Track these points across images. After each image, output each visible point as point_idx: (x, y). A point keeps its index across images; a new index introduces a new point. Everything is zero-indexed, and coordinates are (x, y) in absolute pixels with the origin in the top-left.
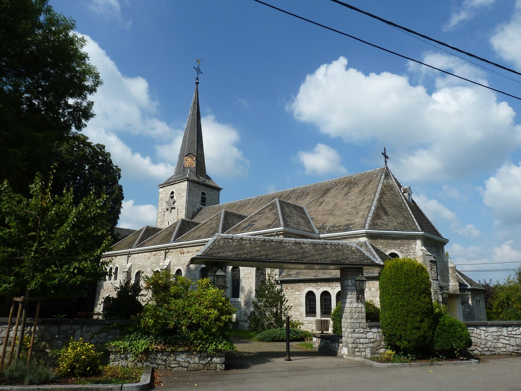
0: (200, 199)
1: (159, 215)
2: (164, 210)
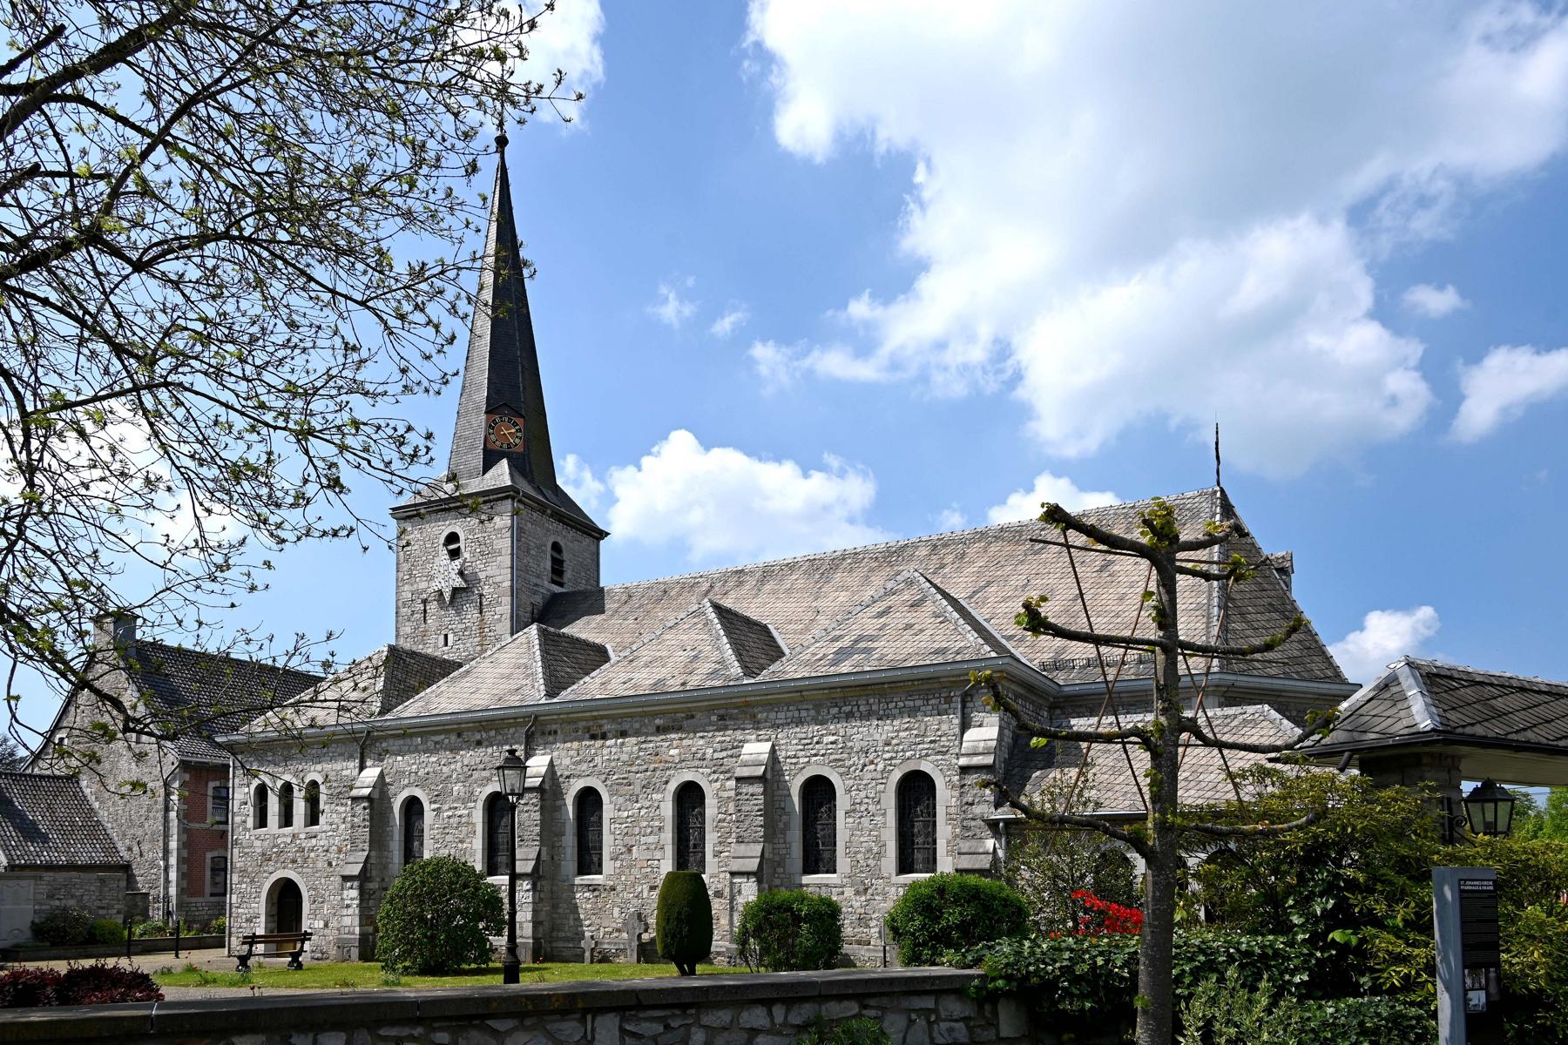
0: (548, 564)
1: (404, 611)
2: (424, 596)
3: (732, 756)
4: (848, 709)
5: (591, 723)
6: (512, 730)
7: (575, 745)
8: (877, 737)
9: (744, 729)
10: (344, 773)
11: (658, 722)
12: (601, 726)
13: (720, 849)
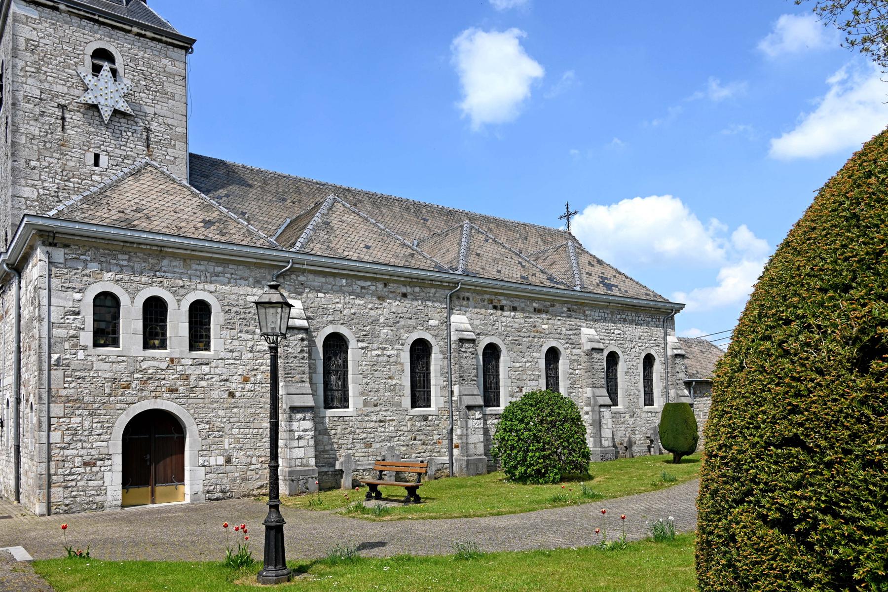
3: (575, 334)
4: (624, 316)
5: (493, 297)
6: (433, 290)
7: (483, 311)
8: (636, 334)
9: (580, 319)
11: (535, 305)
12: (500, 301)
13: (571, 391)
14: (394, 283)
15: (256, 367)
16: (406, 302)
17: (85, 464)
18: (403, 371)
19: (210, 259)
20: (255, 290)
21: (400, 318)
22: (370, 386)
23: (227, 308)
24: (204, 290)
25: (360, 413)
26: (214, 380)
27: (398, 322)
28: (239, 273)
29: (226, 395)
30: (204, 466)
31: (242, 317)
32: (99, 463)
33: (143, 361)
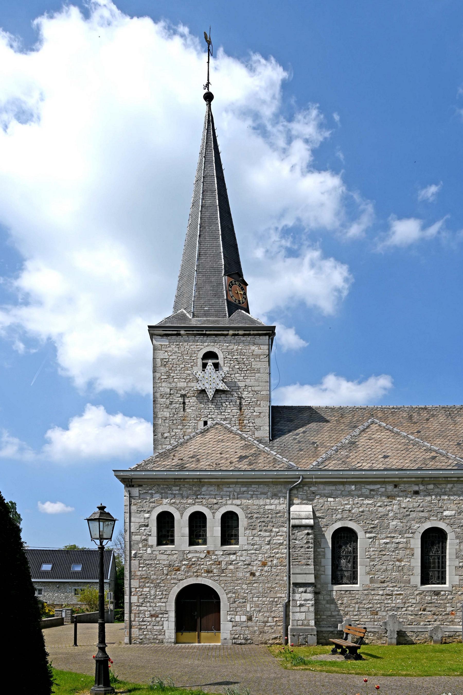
6: (449, 486)
10: (267, 507)
14: (405, 484)
15: (272, 555)
16: (419, 499)
17: (152, 616)
18: (413, 555)
19: (237, 483)
20: (272, 501)
21: (411, 511)
22: (377, 567)
23: (250, 515)
24: (232, 504)
25: (367, 588)
26: (239, 564)
27: (409, 515)
28: (260, 490)
29: (248, 575)
30: (231, 621)
31: (261, 520)
32: (160, 616)
33: (188, 553)
